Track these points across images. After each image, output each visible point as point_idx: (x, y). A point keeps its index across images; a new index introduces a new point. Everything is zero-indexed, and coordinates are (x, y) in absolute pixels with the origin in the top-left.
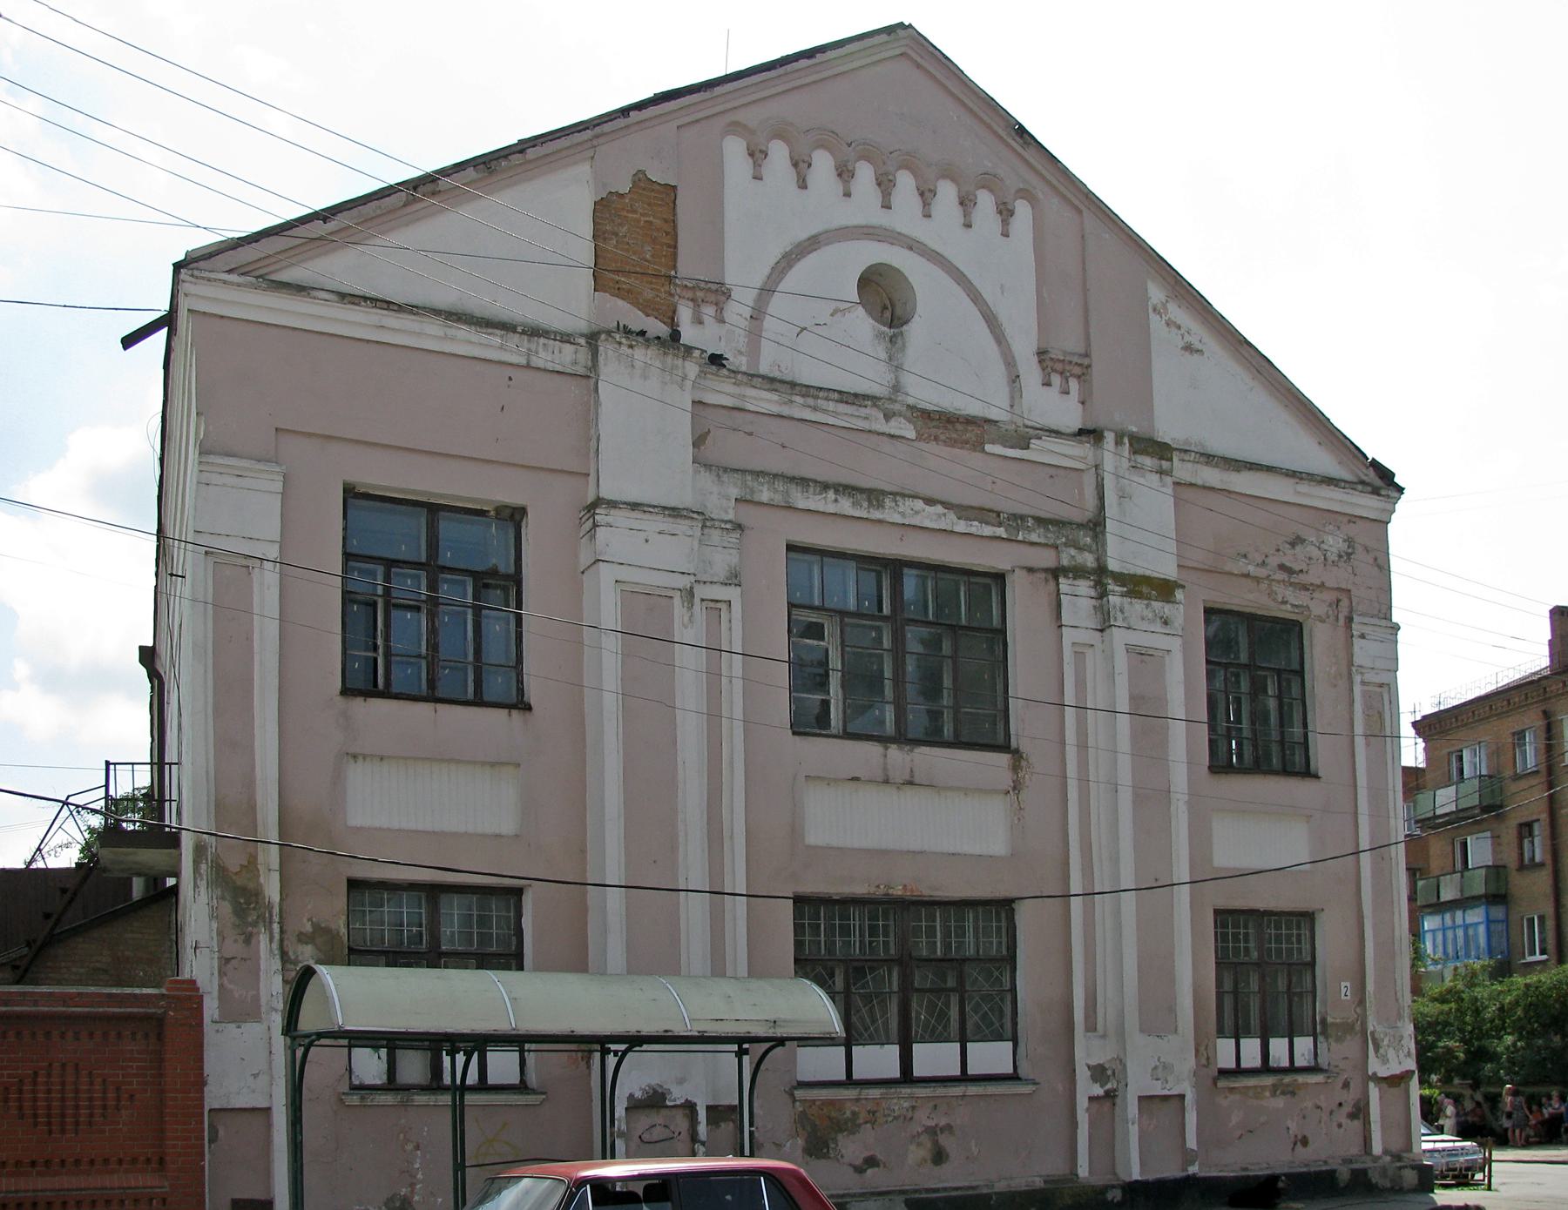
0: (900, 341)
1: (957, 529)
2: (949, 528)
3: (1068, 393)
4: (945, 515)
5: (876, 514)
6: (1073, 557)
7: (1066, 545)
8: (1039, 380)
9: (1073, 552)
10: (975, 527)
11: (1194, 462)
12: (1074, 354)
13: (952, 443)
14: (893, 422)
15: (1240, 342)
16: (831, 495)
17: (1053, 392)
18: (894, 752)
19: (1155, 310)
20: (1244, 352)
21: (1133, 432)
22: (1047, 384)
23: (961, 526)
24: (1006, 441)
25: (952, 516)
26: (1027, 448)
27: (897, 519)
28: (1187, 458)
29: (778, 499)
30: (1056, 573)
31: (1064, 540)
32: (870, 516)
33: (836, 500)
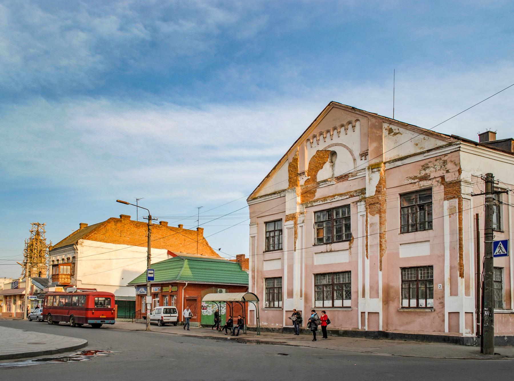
0: (334, 165)
1: (340, 199)
2: (338, 200)
3: (366, 159)
4: (337, 197)
5: (326, 202)
6: (362, 196)
7: (361, 194)
8: (360, 159)
9: (362, 195)
10: (344, 197)
11: (393, 162)
12: (365, 151)
13: (343, 181)
14: (331, 182)
15: (407, 126)
16: (319, 201)
17: (363, 161)
18: (328, 245)
19: (386, 129)
20: (409, 127)
21: (378, 162)
22: (361, 160)
23: (340, 198)
24: (352, 176)
25: (339, 197)
26: (357, 176)
27: (330, 201)
28: (390, 162)
29: (311, 205)
30: (357, 202)
31: (360, 194)
32: (325, 203)
33: (319, 202)
